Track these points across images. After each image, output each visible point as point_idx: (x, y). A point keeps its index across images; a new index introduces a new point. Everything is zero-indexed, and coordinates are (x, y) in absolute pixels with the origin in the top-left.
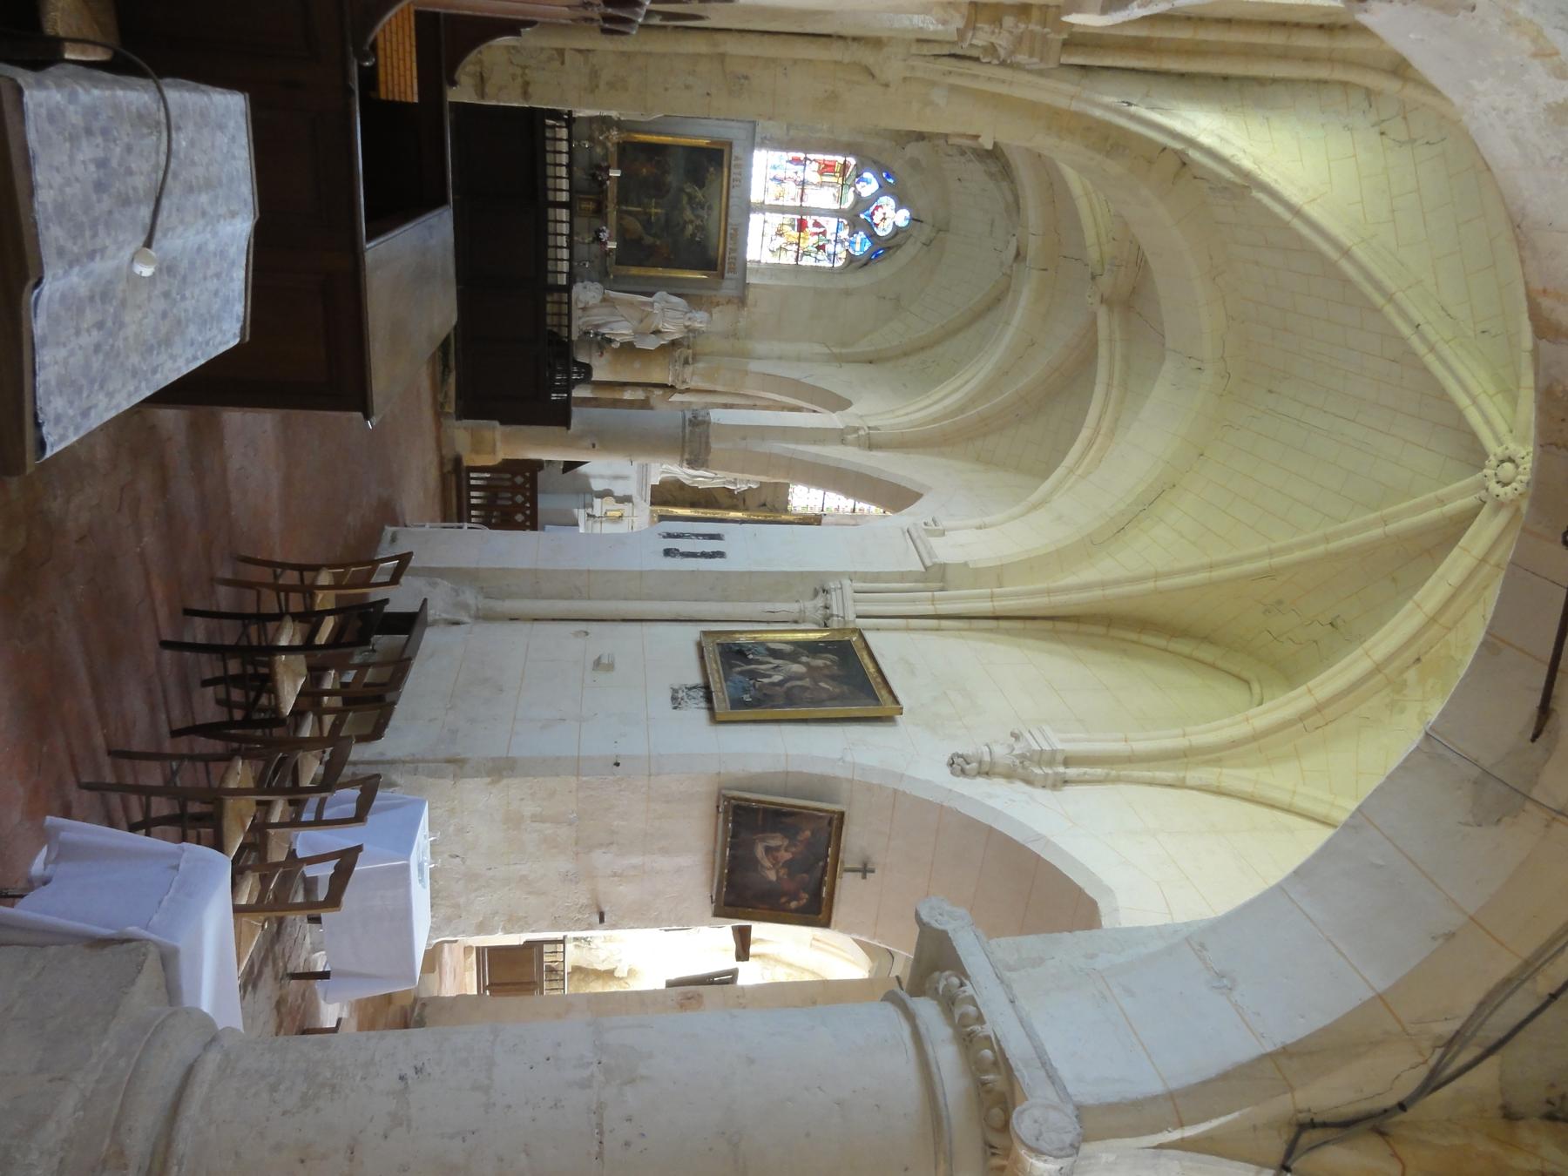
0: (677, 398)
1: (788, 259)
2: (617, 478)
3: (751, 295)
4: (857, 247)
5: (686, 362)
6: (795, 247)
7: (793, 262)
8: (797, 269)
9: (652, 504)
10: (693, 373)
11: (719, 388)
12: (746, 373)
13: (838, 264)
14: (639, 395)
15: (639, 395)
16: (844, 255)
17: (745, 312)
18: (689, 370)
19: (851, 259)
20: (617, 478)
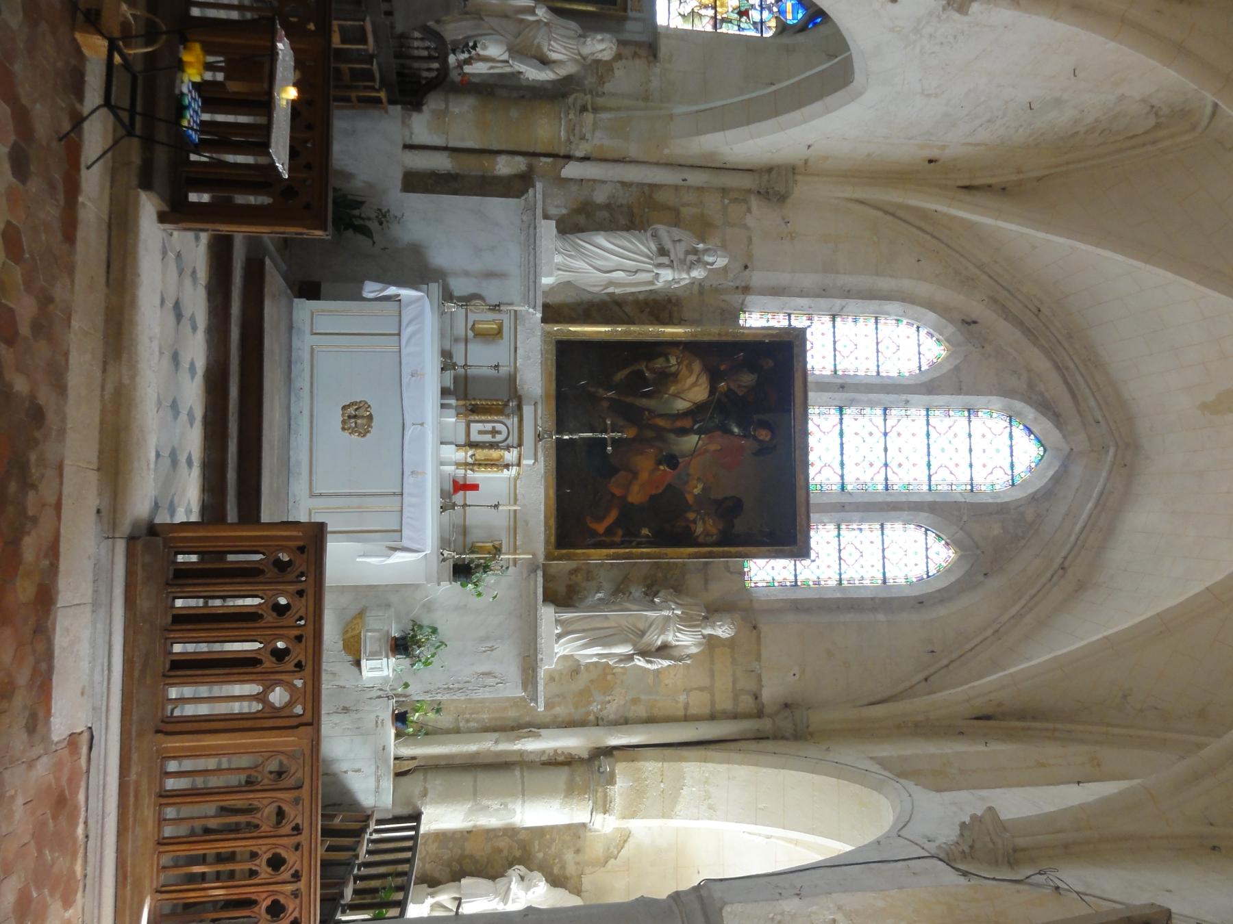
0: (571, 170)
1: (705, 25)
2: (490, 275)
3: (663, 50)
4: (789, 16)
5: (584, 109)
6: (711, 12)
7: (709, 28)
8: (715, 39)
9: (544, 320)
10: (595, 126)
11: (633, 151)
12: (671, 117)
13: (768, 34)
14: (520, 164)
15: (520, 164)
16: (773, 23)
17: (657, 69)
18: (589, 117)
19: (783, 28)
20: (490, 275)
